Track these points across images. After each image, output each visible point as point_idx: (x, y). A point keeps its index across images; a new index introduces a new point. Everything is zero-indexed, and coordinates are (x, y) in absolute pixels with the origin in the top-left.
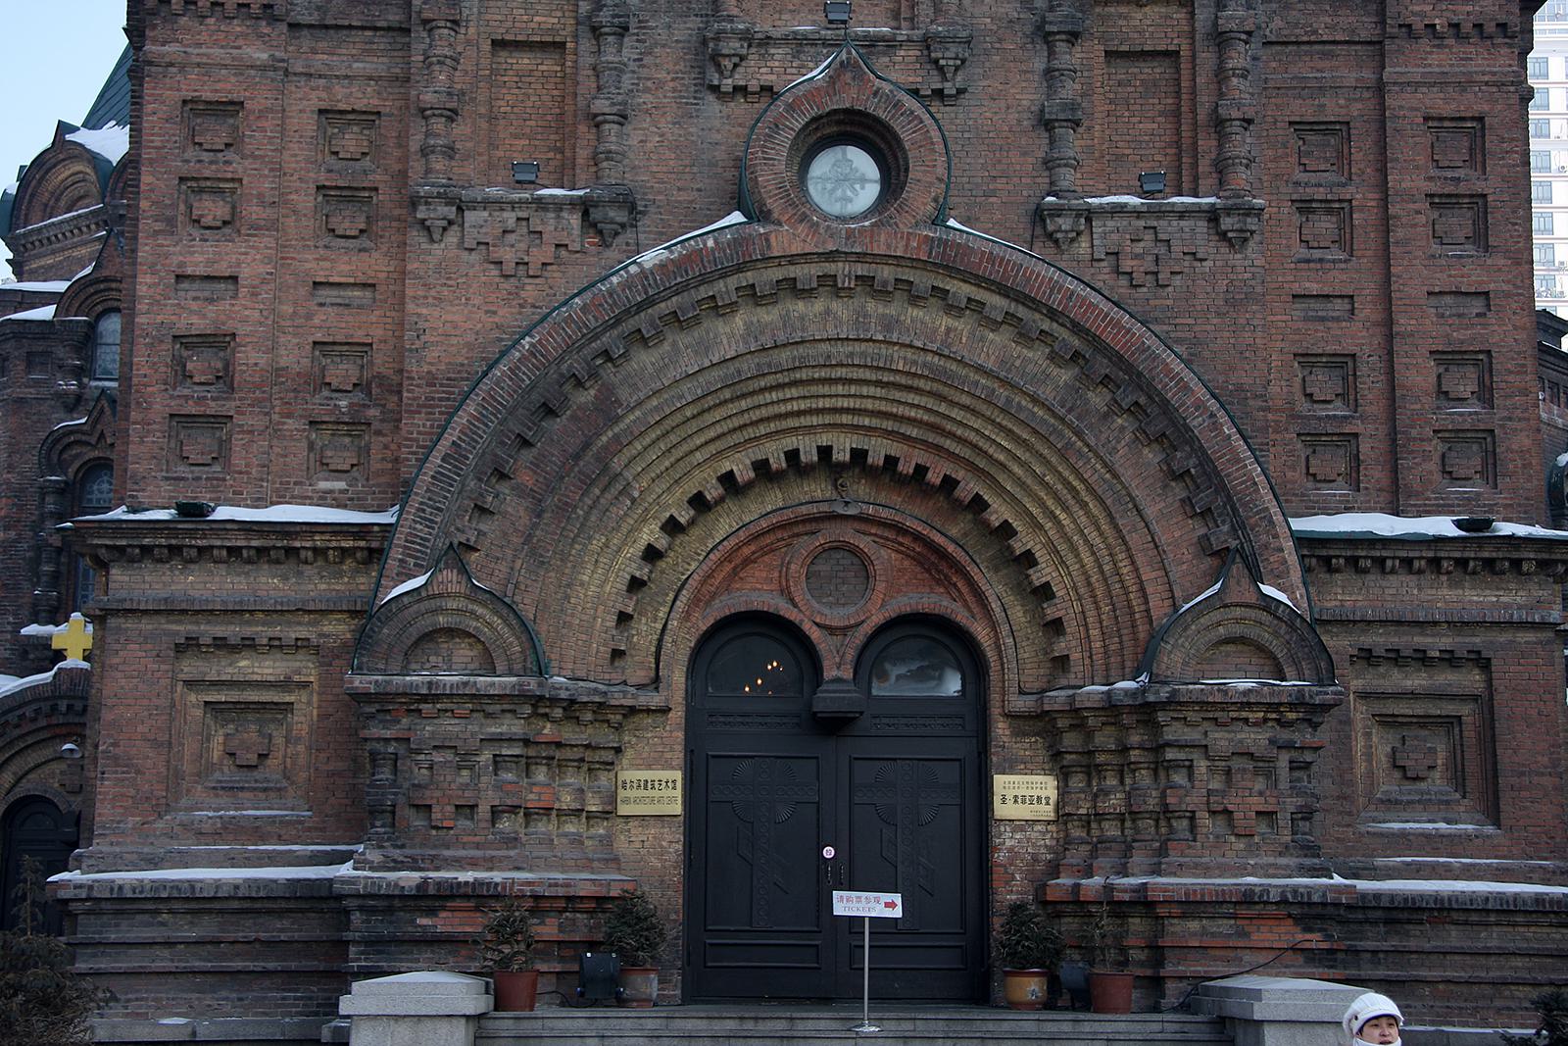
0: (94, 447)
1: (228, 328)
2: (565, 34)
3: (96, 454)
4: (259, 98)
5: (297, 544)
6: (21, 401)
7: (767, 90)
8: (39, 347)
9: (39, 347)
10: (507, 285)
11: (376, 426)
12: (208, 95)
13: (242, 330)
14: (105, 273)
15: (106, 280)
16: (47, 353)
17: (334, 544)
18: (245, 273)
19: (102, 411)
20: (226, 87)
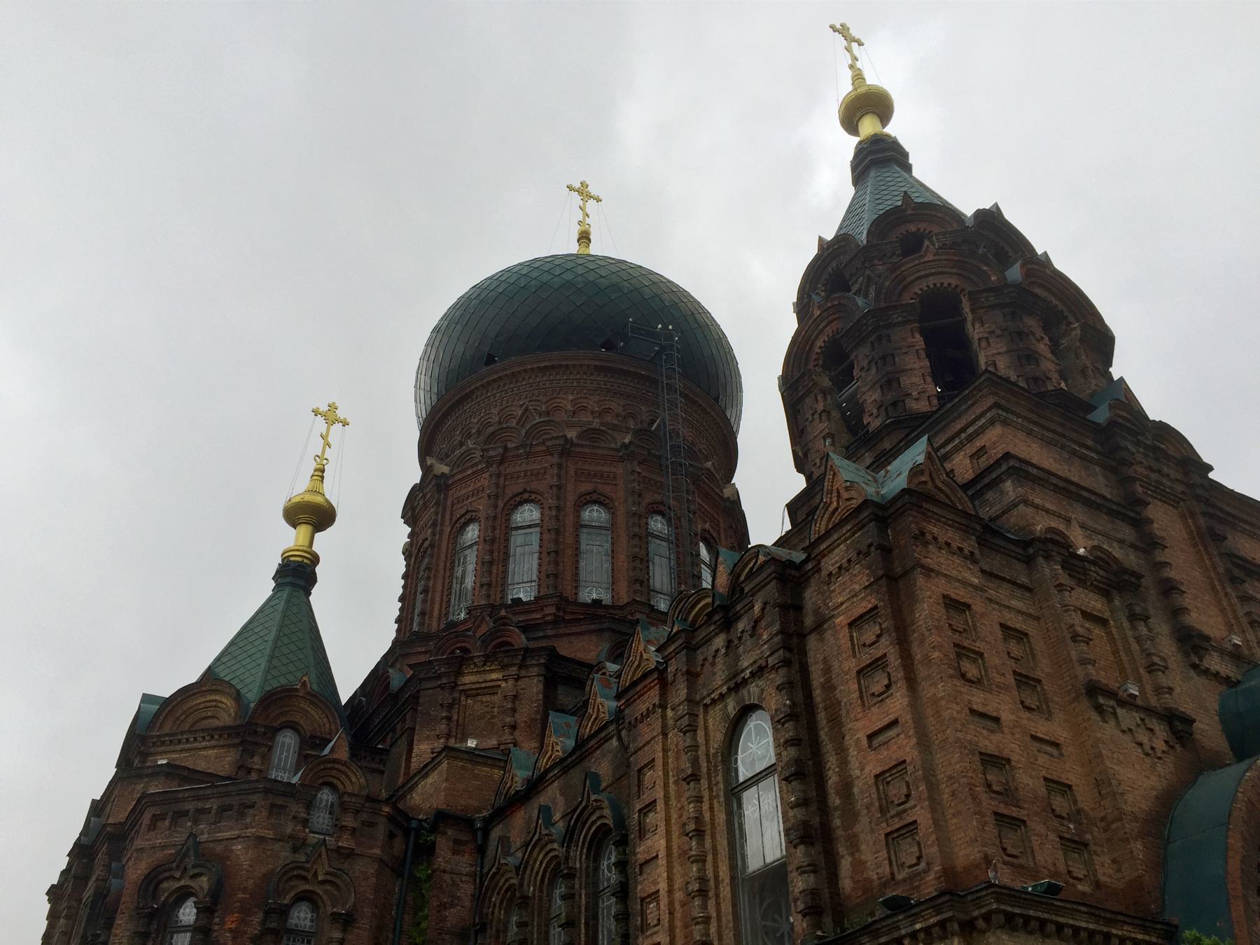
0: (305, 879)
1: (1006, 753)
2: (1107, 615)
3: (307, 887)
4: (978, 606)
5: (1114, 931)
6: (261, 839)
7: (1216, 675)
8: (280, 801)
9: (280, 801)
10: (1148, 760)
11: (1092, 847)
12: (953, 596)
13: (1014, 758)
14: (335, 756)
15: (335, 761)
16: (283, 807)
17: (1133, 935)
18: (1006, 716)
19: (320, 855)
20: (960, 594)
